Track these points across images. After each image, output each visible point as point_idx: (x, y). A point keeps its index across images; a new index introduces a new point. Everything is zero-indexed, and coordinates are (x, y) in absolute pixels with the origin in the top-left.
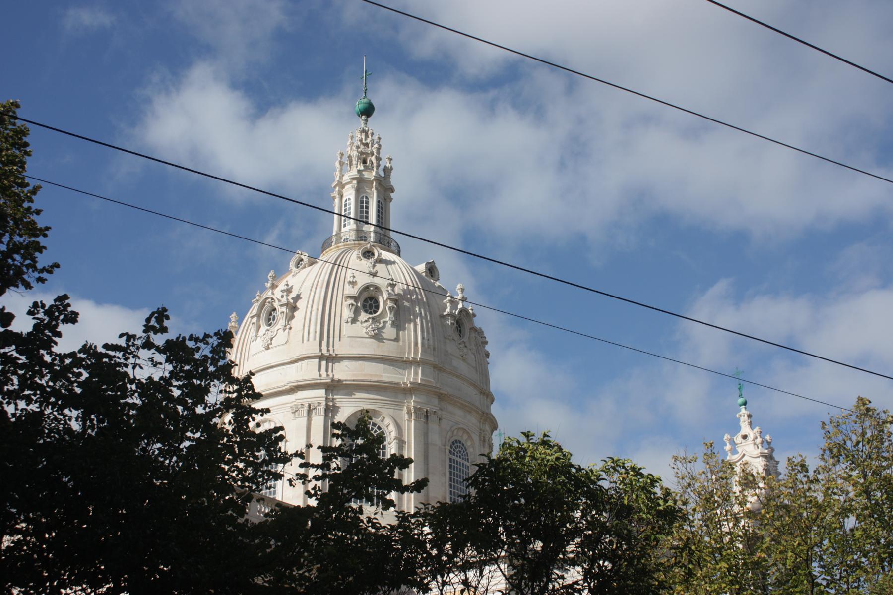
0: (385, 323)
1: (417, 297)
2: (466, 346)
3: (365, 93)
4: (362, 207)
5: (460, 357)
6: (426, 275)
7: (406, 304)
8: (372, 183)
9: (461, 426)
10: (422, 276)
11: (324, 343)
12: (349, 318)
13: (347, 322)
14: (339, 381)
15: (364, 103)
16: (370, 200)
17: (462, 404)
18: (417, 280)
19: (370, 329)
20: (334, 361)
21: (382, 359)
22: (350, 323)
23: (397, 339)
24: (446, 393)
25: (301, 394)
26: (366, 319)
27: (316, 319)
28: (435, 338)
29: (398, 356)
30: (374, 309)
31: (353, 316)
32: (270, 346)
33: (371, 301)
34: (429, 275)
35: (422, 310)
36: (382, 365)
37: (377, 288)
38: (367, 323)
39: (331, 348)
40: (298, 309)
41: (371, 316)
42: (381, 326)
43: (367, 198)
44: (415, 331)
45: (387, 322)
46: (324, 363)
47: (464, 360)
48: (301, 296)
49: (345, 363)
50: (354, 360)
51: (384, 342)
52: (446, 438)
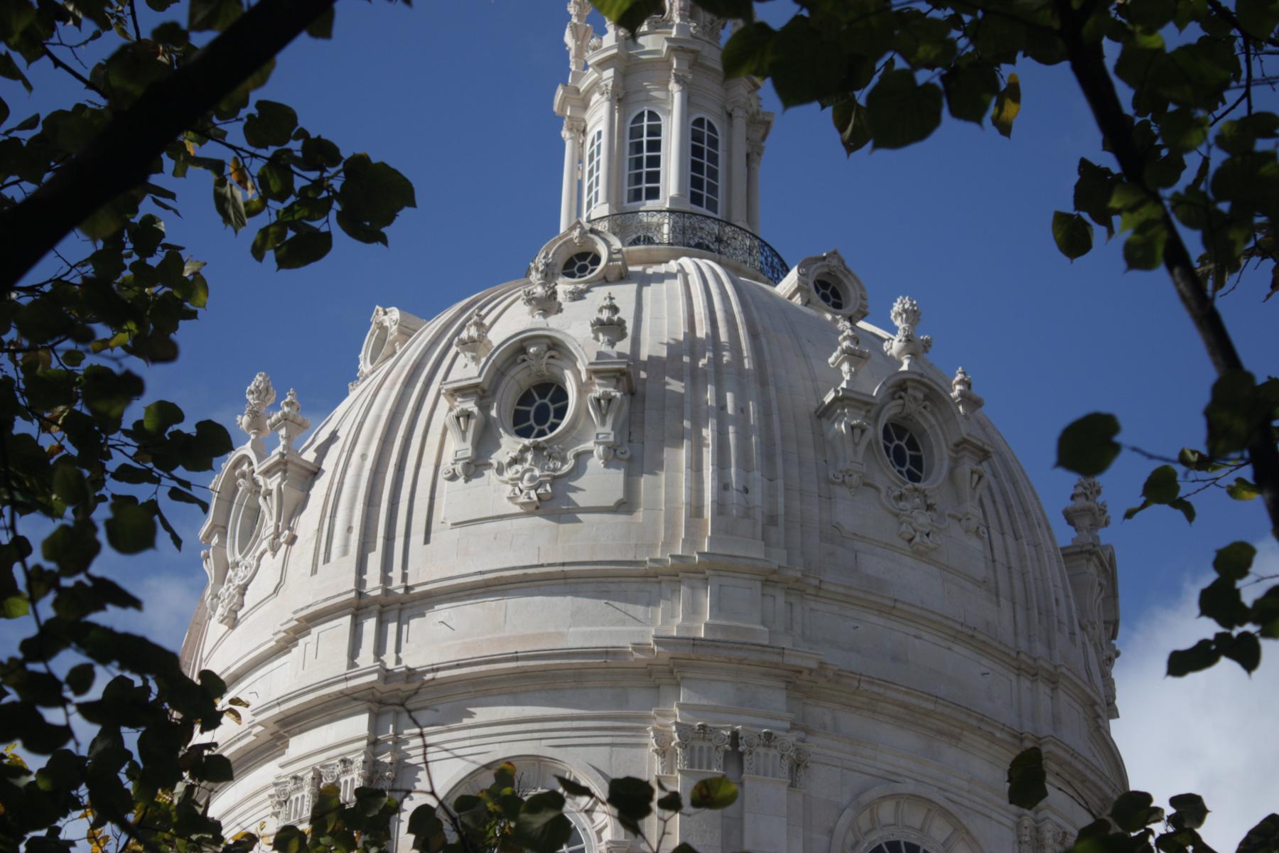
0: (582, 457)
2: (929, 507)
4: (638, 147)
5: (904, 544)
6: (807, 303)
7: (676, 386)
9: (909, 787)
10: (794, 309)
11: (375, 560)
13: (453, 478)
14: (411, 673)
16: (664, 121)
17: (905, 706)
18: (736, 308)
19: (525, 484)
20: (405, 614)
21: (565, 577)
22: (461, 480)
23: (626, 505)
24: (813, 665)
25: (300, 744)
26: (513, 454)
29: (630, 557)
30: (552, 419)
31: (469, 453)
32: (240, 614)
33: (542, 396)
34: (816, 297)
35: (729, 397)
36: (569, 598)
37: (555, 347)
38: (518, 467)
39: (396, 573)
40: (324, 471)
41: (527, 442)
42: (566, 468)
43: (653, 116)
45: (590, 453)
46: (370, 625)
47: (919, 554)
48: (338, 434)
49: (442, 612)
50: (469, 597)
51: (579, 521)
52: (831, 832)
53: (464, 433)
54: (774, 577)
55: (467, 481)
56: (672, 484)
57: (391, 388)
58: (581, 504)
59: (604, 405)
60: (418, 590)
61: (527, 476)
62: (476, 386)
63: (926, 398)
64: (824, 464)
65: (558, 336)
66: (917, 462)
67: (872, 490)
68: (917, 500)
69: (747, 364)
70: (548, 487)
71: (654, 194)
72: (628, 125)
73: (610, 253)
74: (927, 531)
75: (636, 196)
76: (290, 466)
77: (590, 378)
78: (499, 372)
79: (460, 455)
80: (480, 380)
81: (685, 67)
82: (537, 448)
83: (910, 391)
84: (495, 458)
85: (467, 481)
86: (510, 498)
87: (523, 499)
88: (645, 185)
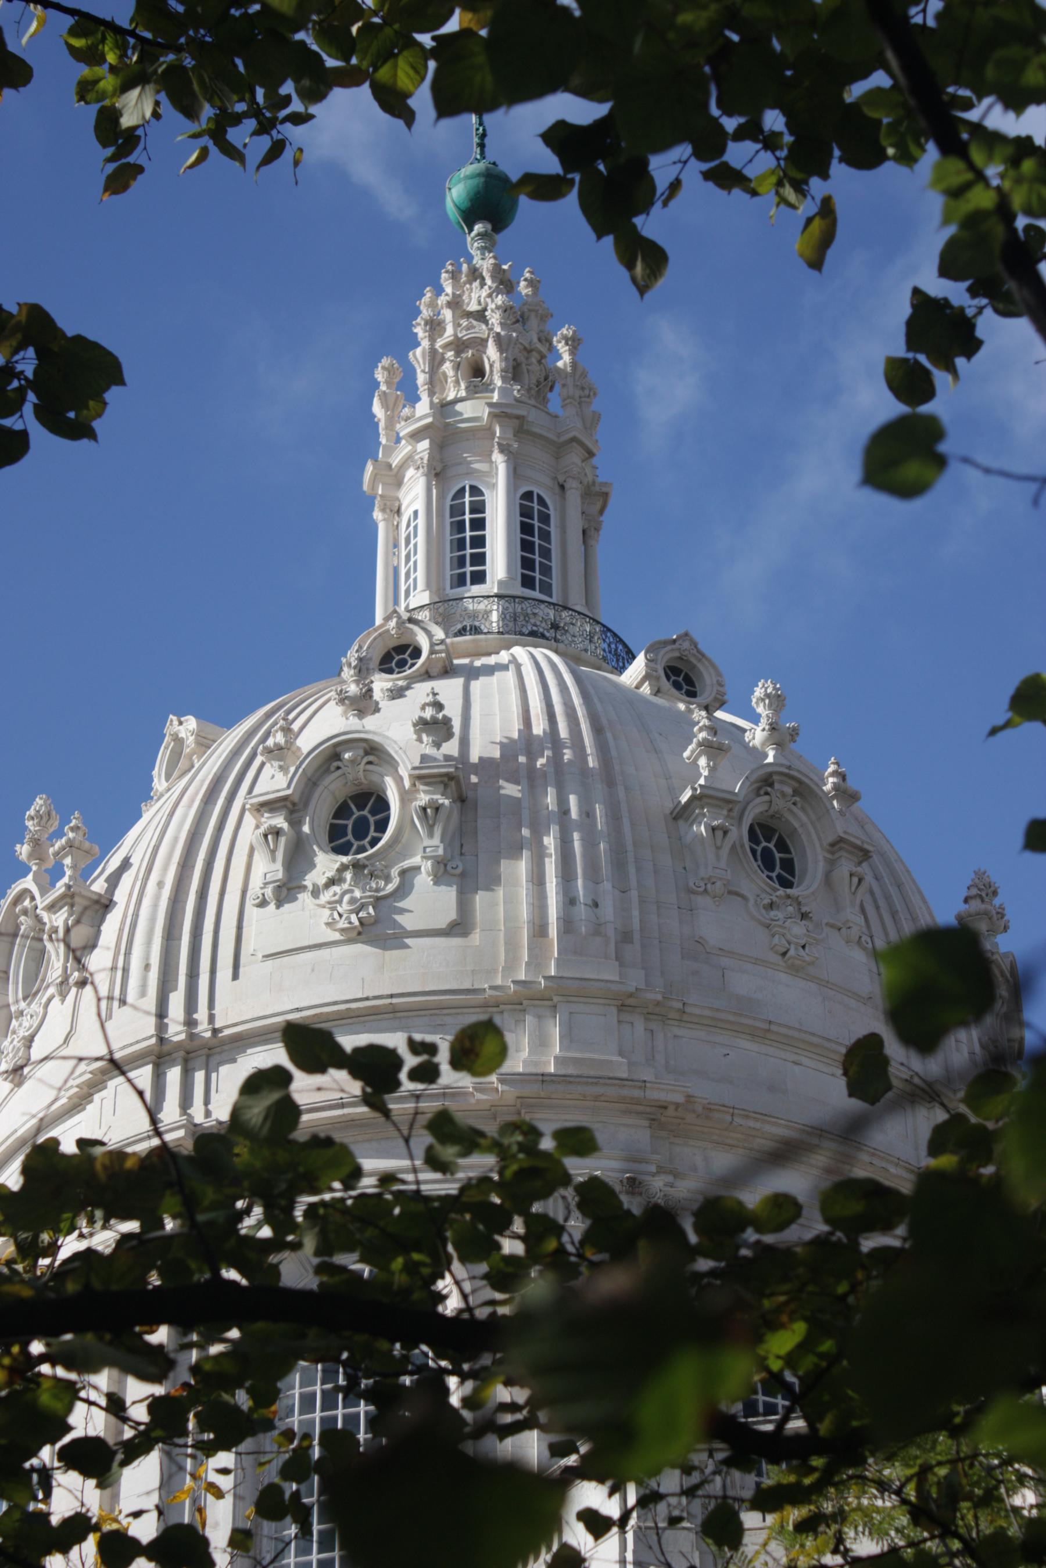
1: (556, 759)
2: (804, 916)
3: (482, 146)
4: (460, 527)
5: (776, 959)
6: (657, 692)
7: (511, 790)
8: (489, 430)
10: (642, 699)
12: (266, 884)
13: (263, 903)
15: (467, 178)
19: (344, 907)
20: (213, 1061)
22: (272, 906)
23: (460, 927)
24: (680, 1099)
26: (330, 874)
27: (153, 919)
28: (634, 894)
29: (467, 985)
30: (372, 833)
31: (280, 875)
33: (361, 807)
34: (666, 685)
35: (573, 800)
38: (336, 889)
39: (201, 1015)
40: (116, 903)
41: (345, 859)
42: (390, 887)
43: (475, 491)
44: (538, 880)
45: (417, 869)
46: (174, 1075)
47: (796, 970)
48: (131, 861)
51: (407, 947)
53: (273, 852)
54: (631, 1001)
55: (278, 907)
56: (511, 901)
57: (190, 806)
58: (409, 927)
59: (430, 814)
60: (227, 1032)
61: (346, 898)
62: (285, 798)
63: (796, 792)
64: (684, 871)
65: (376, 738)
66: (788, 865)
67: (739, 899)
68: (790, 909)
69: (592, 762)
70: (371, 910)
71: (479, 578)
72: (448, 502)
73: (432, 645)
74: (803, 942)
75: (460, 581)
76: (77, 899)
77: (414, 785)
78: (311, 782)
79: (269, 877)
80: (289, 792)
81: (510, 435)
82: (357, 866)
83: (777, 786)
84: (309, 880)
85: (278, 907)
86: (328, 924)
87: (342, 924)
88: (469, 569)
